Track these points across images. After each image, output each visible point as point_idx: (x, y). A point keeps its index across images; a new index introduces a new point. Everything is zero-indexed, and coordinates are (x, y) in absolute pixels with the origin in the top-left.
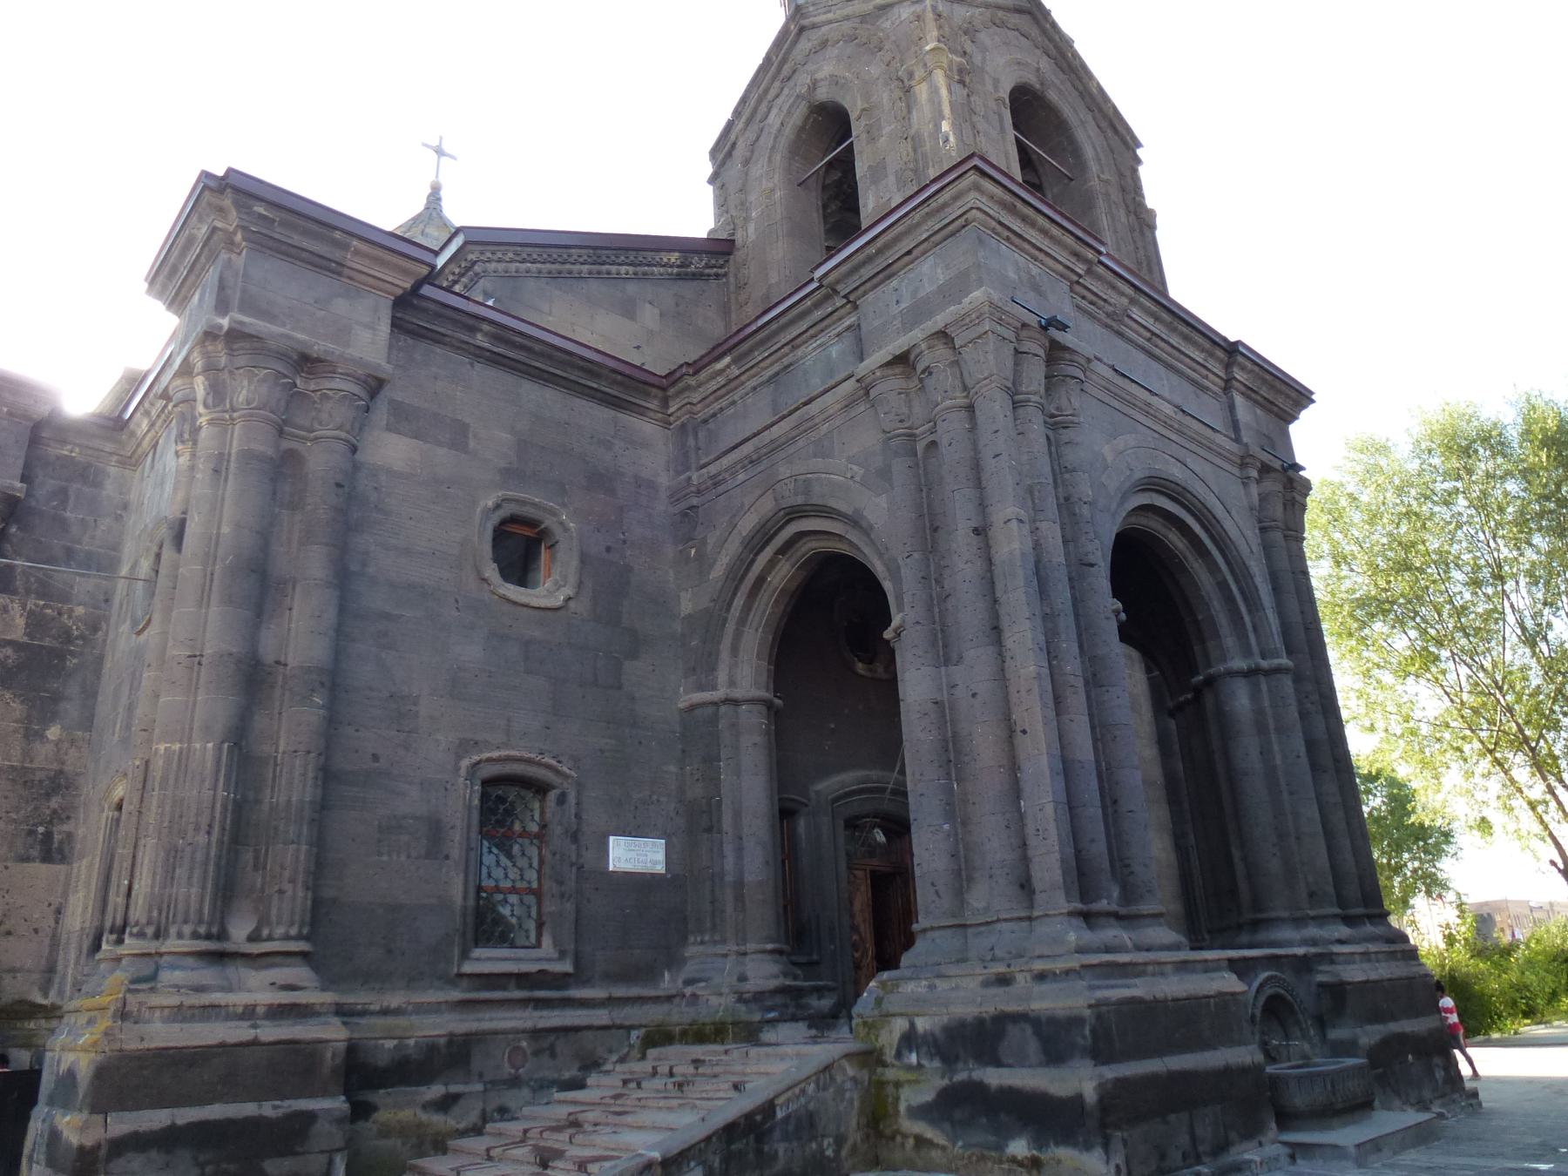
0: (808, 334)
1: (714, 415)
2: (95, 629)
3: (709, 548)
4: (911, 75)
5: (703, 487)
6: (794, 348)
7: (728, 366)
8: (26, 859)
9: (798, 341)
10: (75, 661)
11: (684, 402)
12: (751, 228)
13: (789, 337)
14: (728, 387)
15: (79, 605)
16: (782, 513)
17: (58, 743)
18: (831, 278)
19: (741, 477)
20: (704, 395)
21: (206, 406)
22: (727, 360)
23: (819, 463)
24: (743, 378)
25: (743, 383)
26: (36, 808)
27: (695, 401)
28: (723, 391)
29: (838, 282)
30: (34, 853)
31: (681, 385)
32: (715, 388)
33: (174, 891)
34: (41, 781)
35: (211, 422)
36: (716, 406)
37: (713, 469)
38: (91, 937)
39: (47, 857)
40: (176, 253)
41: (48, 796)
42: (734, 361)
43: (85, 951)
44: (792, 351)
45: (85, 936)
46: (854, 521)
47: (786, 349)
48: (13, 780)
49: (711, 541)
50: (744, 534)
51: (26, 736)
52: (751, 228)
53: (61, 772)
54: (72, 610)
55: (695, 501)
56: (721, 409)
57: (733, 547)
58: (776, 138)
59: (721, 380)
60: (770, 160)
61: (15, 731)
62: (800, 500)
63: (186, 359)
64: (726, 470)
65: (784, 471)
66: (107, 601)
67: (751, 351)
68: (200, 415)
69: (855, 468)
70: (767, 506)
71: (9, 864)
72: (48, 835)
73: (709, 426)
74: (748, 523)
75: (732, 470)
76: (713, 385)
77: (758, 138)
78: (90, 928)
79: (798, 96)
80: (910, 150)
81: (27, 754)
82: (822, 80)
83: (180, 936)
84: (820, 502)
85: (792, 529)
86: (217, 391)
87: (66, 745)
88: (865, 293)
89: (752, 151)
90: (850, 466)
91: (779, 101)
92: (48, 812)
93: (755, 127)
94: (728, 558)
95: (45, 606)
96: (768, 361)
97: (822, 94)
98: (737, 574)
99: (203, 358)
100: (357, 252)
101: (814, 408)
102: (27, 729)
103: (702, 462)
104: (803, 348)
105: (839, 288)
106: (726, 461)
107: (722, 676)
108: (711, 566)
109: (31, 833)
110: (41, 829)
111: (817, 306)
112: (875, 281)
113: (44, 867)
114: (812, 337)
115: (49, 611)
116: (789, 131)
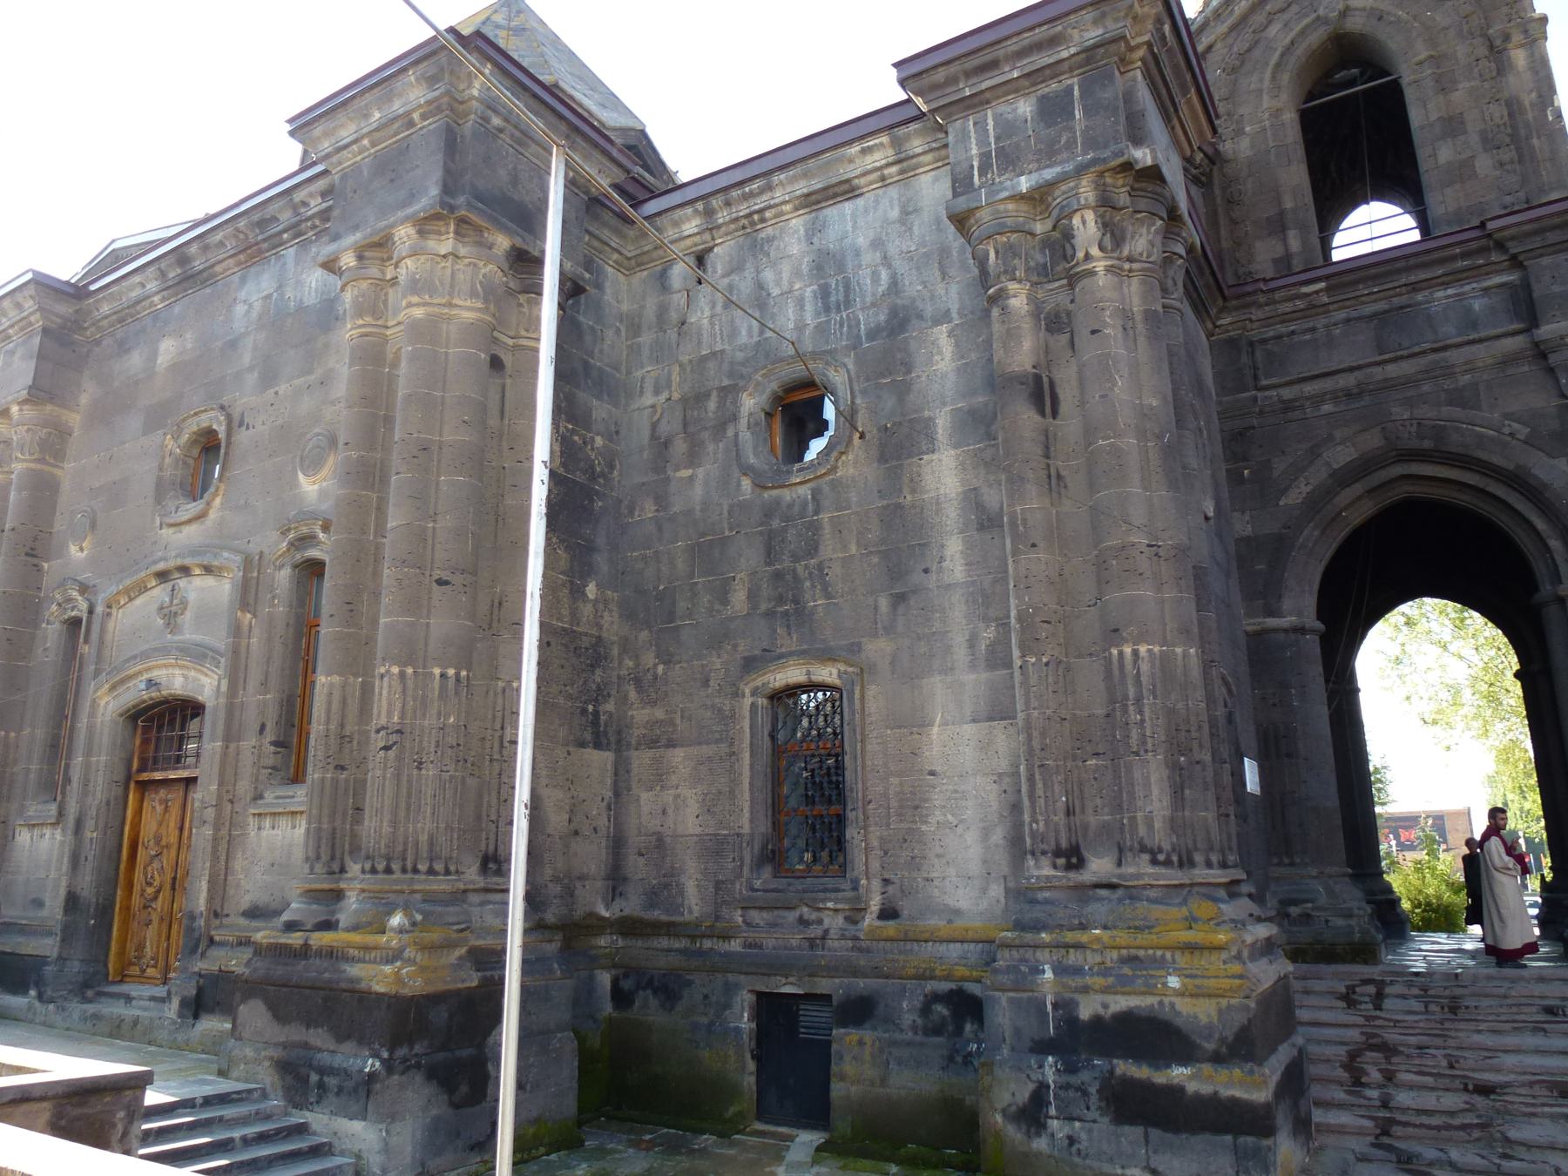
0: (1439, 281)
1: (1279, 337)
2: (612, 467)
3: (1276, 474)
4: (1507, 38)
5: (1268, 409)
6: (1415, 290)
7: (1317, 292)
8: (582, 744)
9: (1425, 284)
10: (600, 504)
11: (1243, 317)
12: (1245, 143)
13: (1413, 278)
14: (1307, 313)
15: (598, 434)
16: (1394, 453)
17: (596, 602)
18: (1506, 233)
19: (1327, 408)
20: (1269, 315)
21: (1101, 248)
22: (1322, 285)
23: (1457, 412)
24: (1331, 307)
25: (1329, 312)
26: (585, 682)
27: (1254, 318)
28: (1299, 314)
29: (1513, 238)
30: (588, 736)
31: (1249, 299)
32: (1288, 310)
33: (1187, 813)
34: (587, 649)
35: (1109, 269)
36: (1282, 329)
37: (1287, 393)
38: (757, 847)
39: (598, 746)
40: (1012, 46)
41: (593, 667)
42: (1327, 289)
43: (747, 860)
44: (1408, 293)
45: (744, 845)
46: (1518, 480)
47: (1404, 290)
48: (566, 646)
49: (1279, 466)
50: (1336, 466)
51: (571, 592)
52: (1245, 143)
53: (599, 638)
54: (593, 440)
55: (1255, 422)
56: (1293, 333)
57: (1317, 475)
58: (1283, 55)
59: (1300, 304)
60: (1274, 78)
61: (563, 585)
62: (1427, 444)
63: (1051, 185)
64: (1307, 398)
65: (1400, 412)
66: (617, 433)
67: (1357, 282)
68: (1088, 257)
69: (1515, 425)
70: (1373, 441)
71: (571, 749)
72: (596, 714)
73: (1269, 347)
74: (1341, 455)
75: (1318, 400)
76: (1287, 307)
77: (1249, 50)
78: (752, 835)
79: (1318, 18)
80: (1506, 114)
81: (574, 615)
82: (1356, 9)
83: (1209, 865)
84: (1461, 450)
85: (1398, 470)
86: (1113, 235)
87: (601, 606)
88: (1541, 255)
89: (1242, 63)
90: (1507, 422)
91: (1286, 16)
92: (594, 687)
93: (1246, 38)
94: (1310, 488)
95: (573, 432)
96: (1374, 297)
97: (1355, 24)
98: (1315, 503)
99: (1096, 189)
100: (1189, 102)
101: (1454, 356)
102: (572, 583)
103: (1264, 382)
104: (1426, 293)
105: (1510, 244)
106: (1309, 388)
107: (1287, 604)
108: (1284, 491)
109: (584, 711)
110: (590, 708)
111: (1464, 256)
112: (1558, 247)
113: (596, 752)
114: (1443, 284)
115: (576, 438)
116: (1301, 50)
